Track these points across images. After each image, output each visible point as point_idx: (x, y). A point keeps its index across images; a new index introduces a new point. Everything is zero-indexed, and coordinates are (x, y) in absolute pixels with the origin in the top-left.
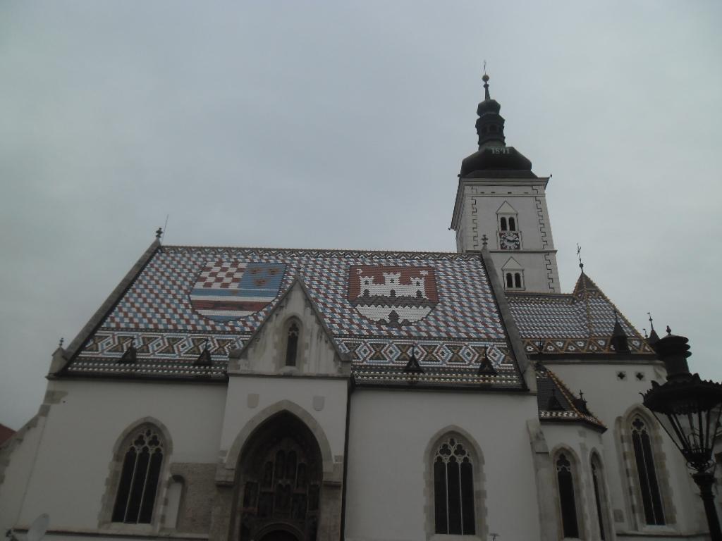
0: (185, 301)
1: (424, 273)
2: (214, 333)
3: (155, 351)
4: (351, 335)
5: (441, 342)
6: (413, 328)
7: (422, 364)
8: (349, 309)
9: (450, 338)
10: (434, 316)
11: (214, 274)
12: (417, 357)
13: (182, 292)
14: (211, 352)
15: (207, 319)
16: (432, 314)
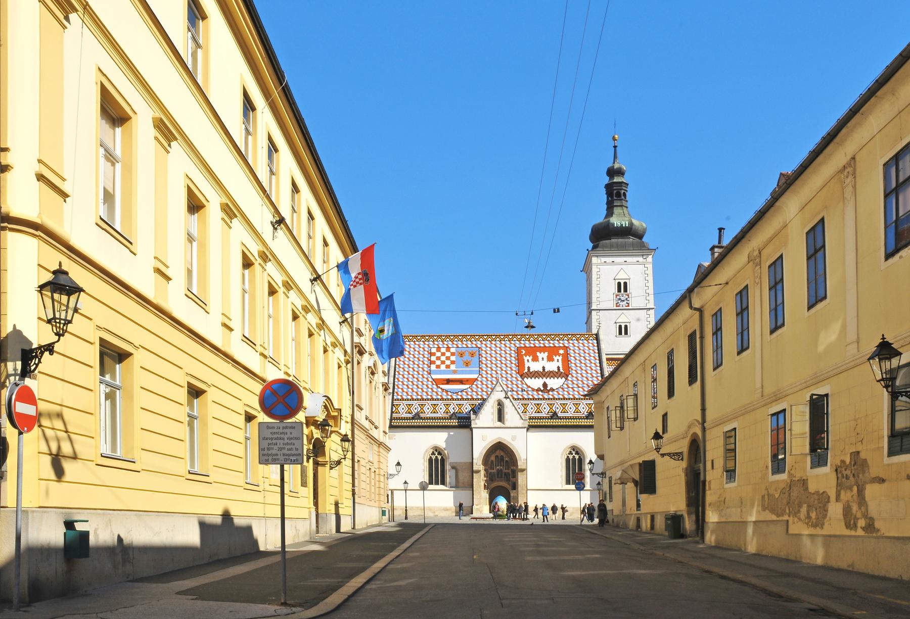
0: (430, 380)
1: (561, 352)
2: (453, 400)
3: (428, 412)
4: (524, 399)
5: (570, 401)
6: (555, 393)
7: (560, 415)
8: (521, 381)
9: (574, 399)
10: (567, 385)
11: (438, 358)
12: (557, 410)
13: (426, 373)
14: (456, 411)
15: (447, 391)
16: (566, 383)
